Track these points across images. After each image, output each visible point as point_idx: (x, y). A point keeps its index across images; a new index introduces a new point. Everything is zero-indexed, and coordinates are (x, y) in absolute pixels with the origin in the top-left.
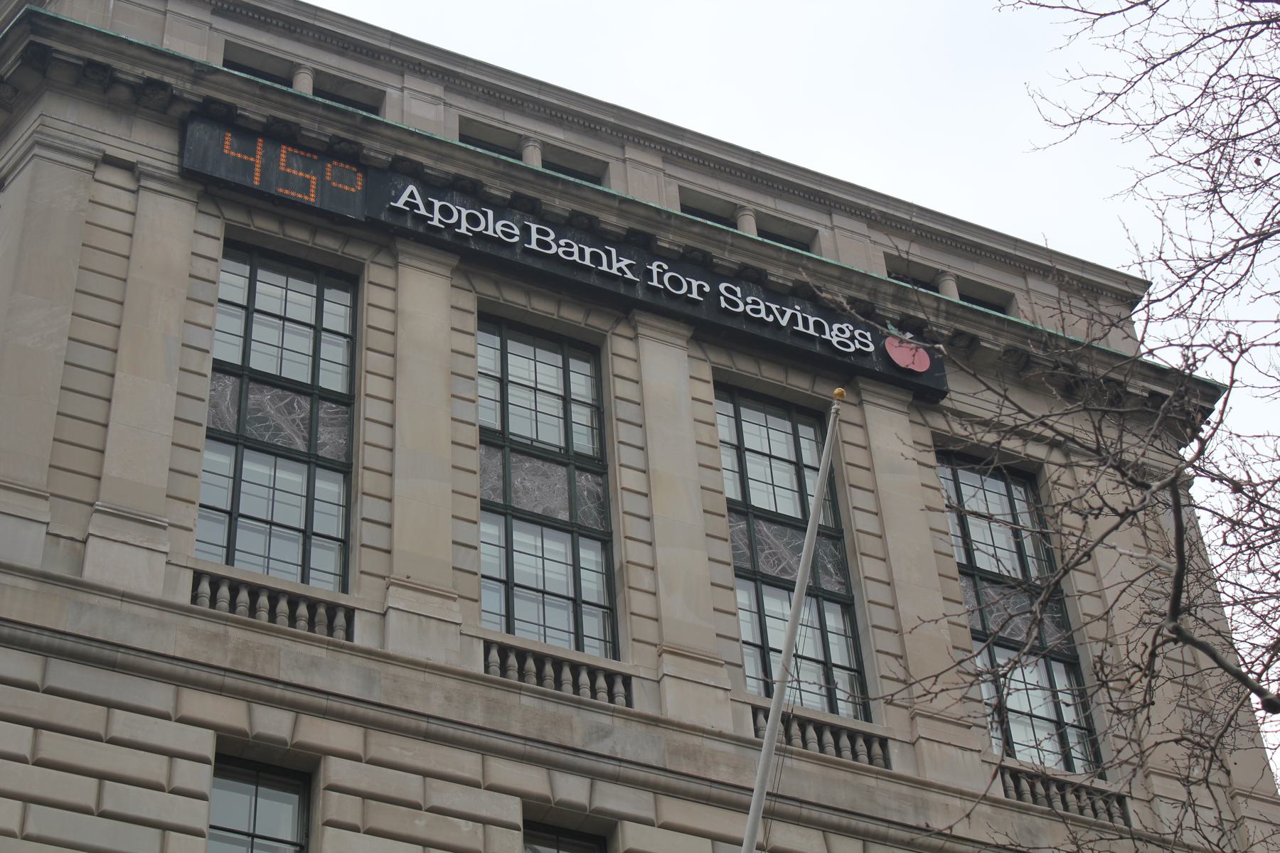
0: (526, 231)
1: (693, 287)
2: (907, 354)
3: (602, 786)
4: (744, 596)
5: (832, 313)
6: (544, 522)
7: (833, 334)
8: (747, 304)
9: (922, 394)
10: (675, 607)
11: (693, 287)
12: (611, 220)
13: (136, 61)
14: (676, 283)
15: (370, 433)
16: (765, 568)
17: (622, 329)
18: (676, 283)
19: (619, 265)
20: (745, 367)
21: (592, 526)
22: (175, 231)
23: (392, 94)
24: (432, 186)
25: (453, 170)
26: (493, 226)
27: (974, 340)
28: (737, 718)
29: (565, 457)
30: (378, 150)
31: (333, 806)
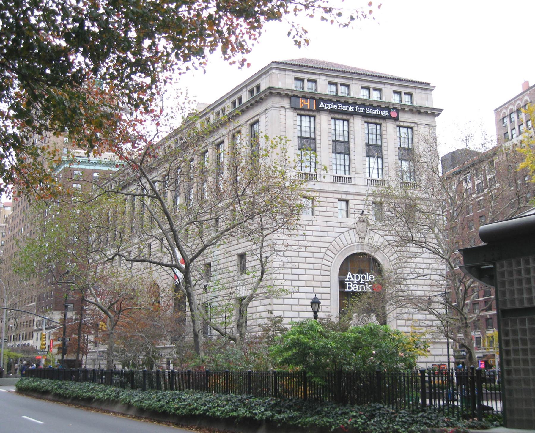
0: (338, 106)
1: (362, 110)
2: (394, 114)
3: (348, 195)
4: (367, 159)
5: (383, 109)
6: (340, 153)
7: (382, 114)
8: (371, 111)
9: (397, 119)
10: (357, 166)
11: (362, 110)
12: (350, 101)
13: (284, 91)
14: (359, 110)
15: (318, 145)
16: (371, 154)
17: (352, 118)
18: (359, 110)
19: (351, 109)
20: (369, 120)
21: (347, 152)
22: (291, 116)
23: (318, 80)
24: (325, 101)
25: (327, 98)
26: (334, 107)
27: (404, 109)
28: (365, 182)
29: (344, 142)
30: (317, 97)
31: (316, 203)
